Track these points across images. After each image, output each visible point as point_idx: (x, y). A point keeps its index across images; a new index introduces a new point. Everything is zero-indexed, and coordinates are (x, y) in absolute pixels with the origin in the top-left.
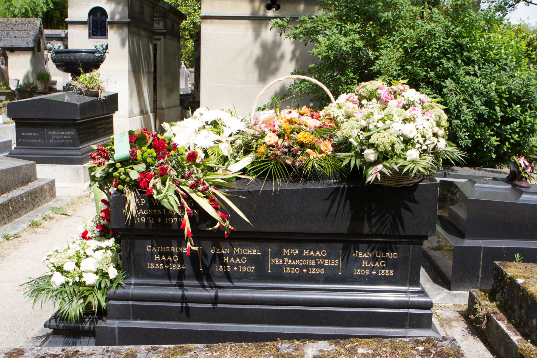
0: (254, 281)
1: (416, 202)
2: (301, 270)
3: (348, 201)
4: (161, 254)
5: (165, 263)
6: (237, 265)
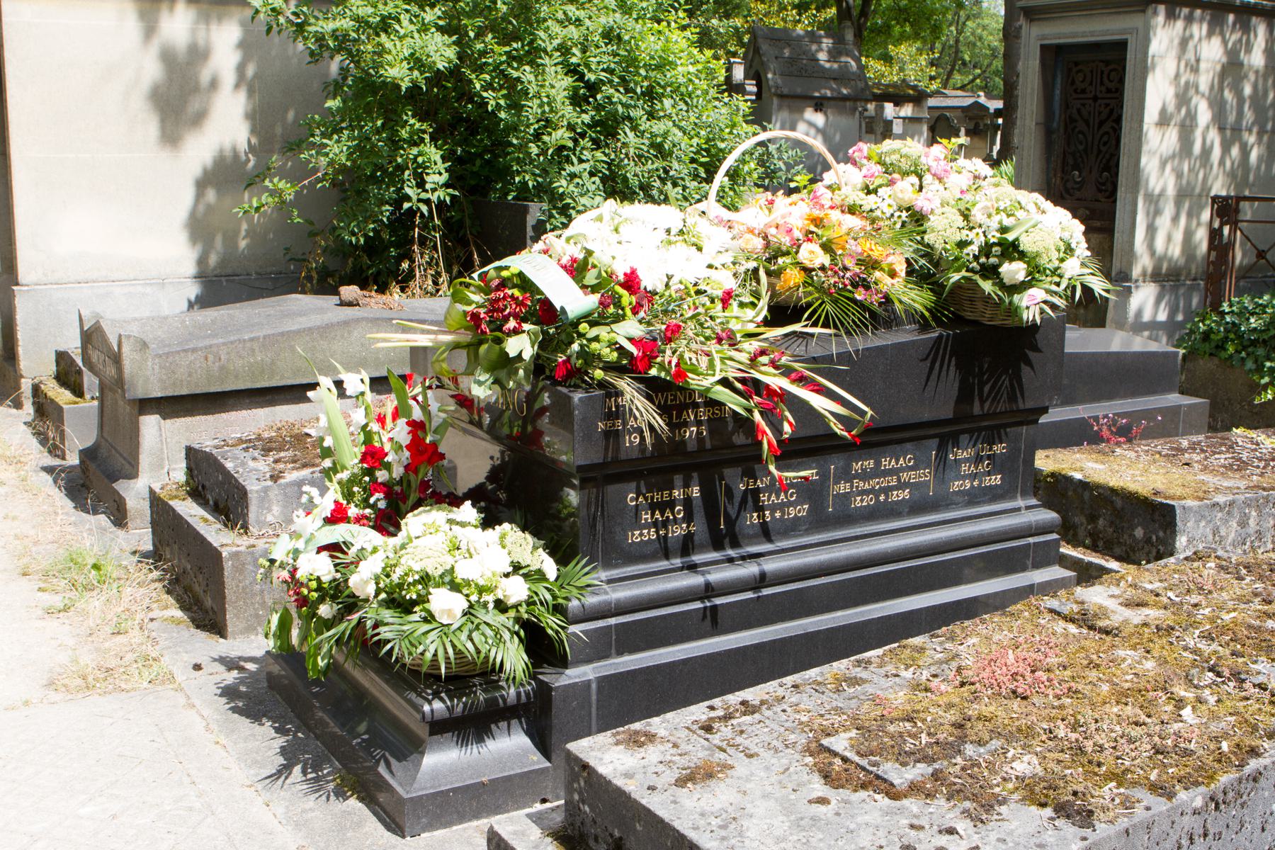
0: (808, 532)
1: (1038, 350)
2: (877, 497)
3: (954, 359)
4: (653, 507)
5: (660, 525)
6: (782, 507)
